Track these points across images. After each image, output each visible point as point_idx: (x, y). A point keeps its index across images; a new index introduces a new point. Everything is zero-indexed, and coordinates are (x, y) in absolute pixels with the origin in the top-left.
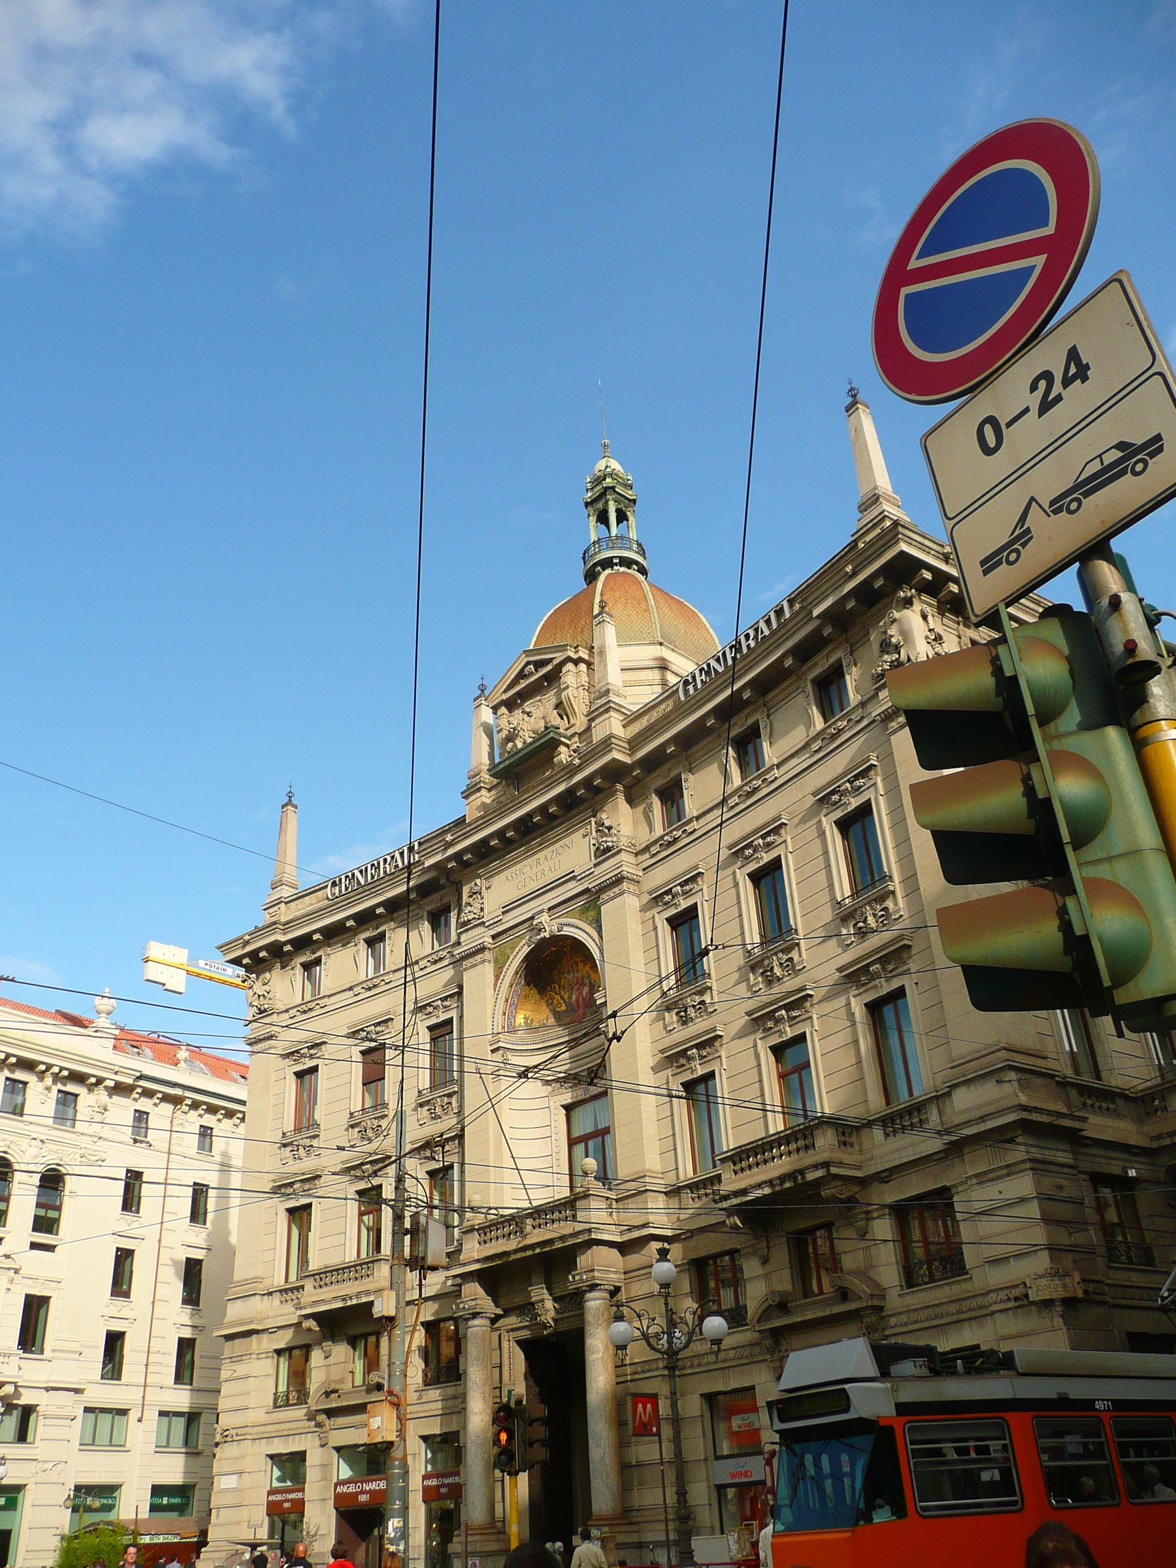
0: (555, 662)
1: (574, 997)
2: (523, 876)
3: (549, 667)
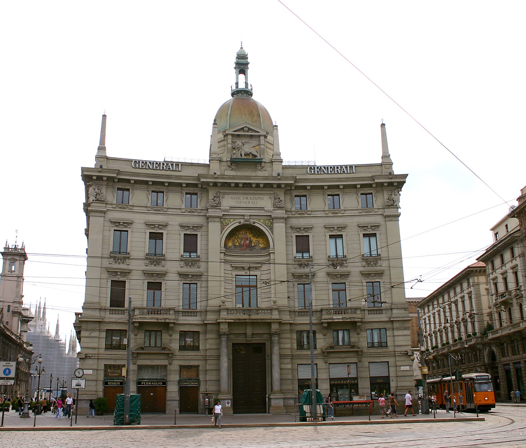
0: (259, 134)
1: (242, 243)
2: (239, 200)
3: (257, 134)
